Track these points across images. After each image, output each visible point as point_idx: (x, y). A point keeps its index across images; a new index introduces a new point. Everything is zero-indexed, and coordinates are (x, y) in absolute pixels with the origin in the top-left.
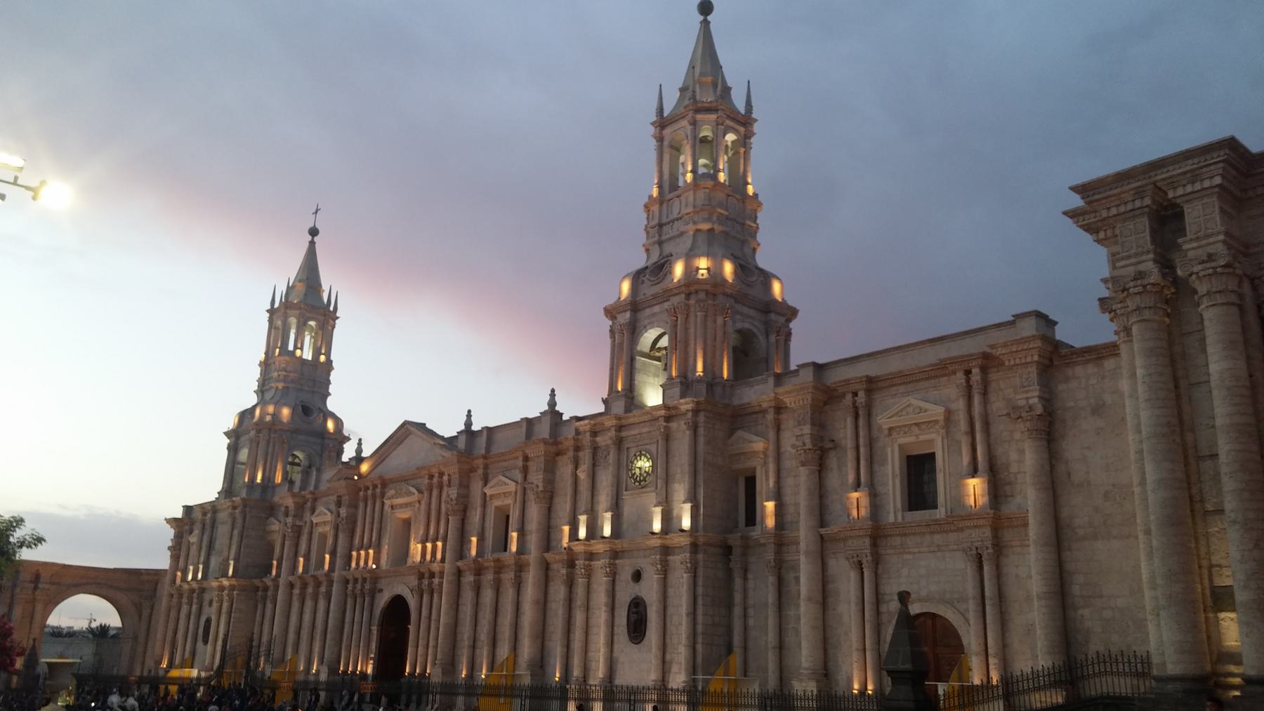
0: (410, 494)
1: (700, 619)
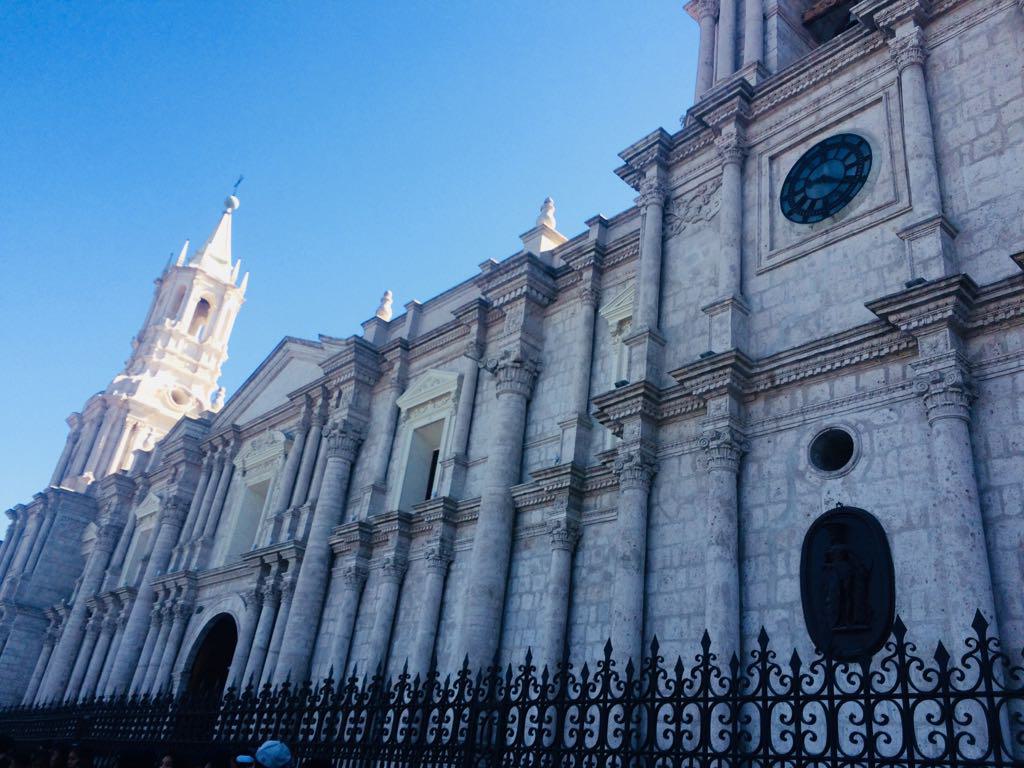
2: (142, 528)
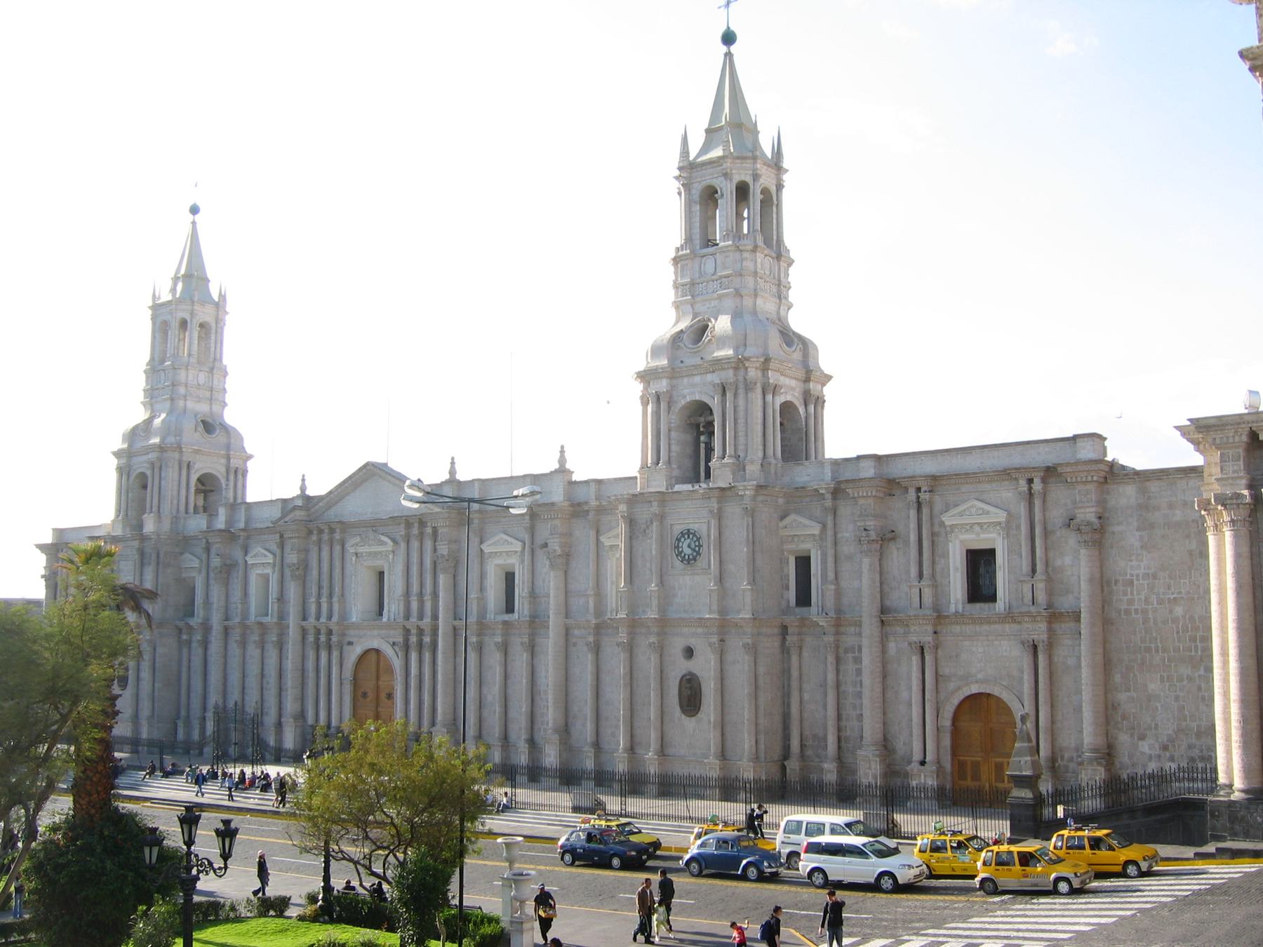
0: (383, 543)
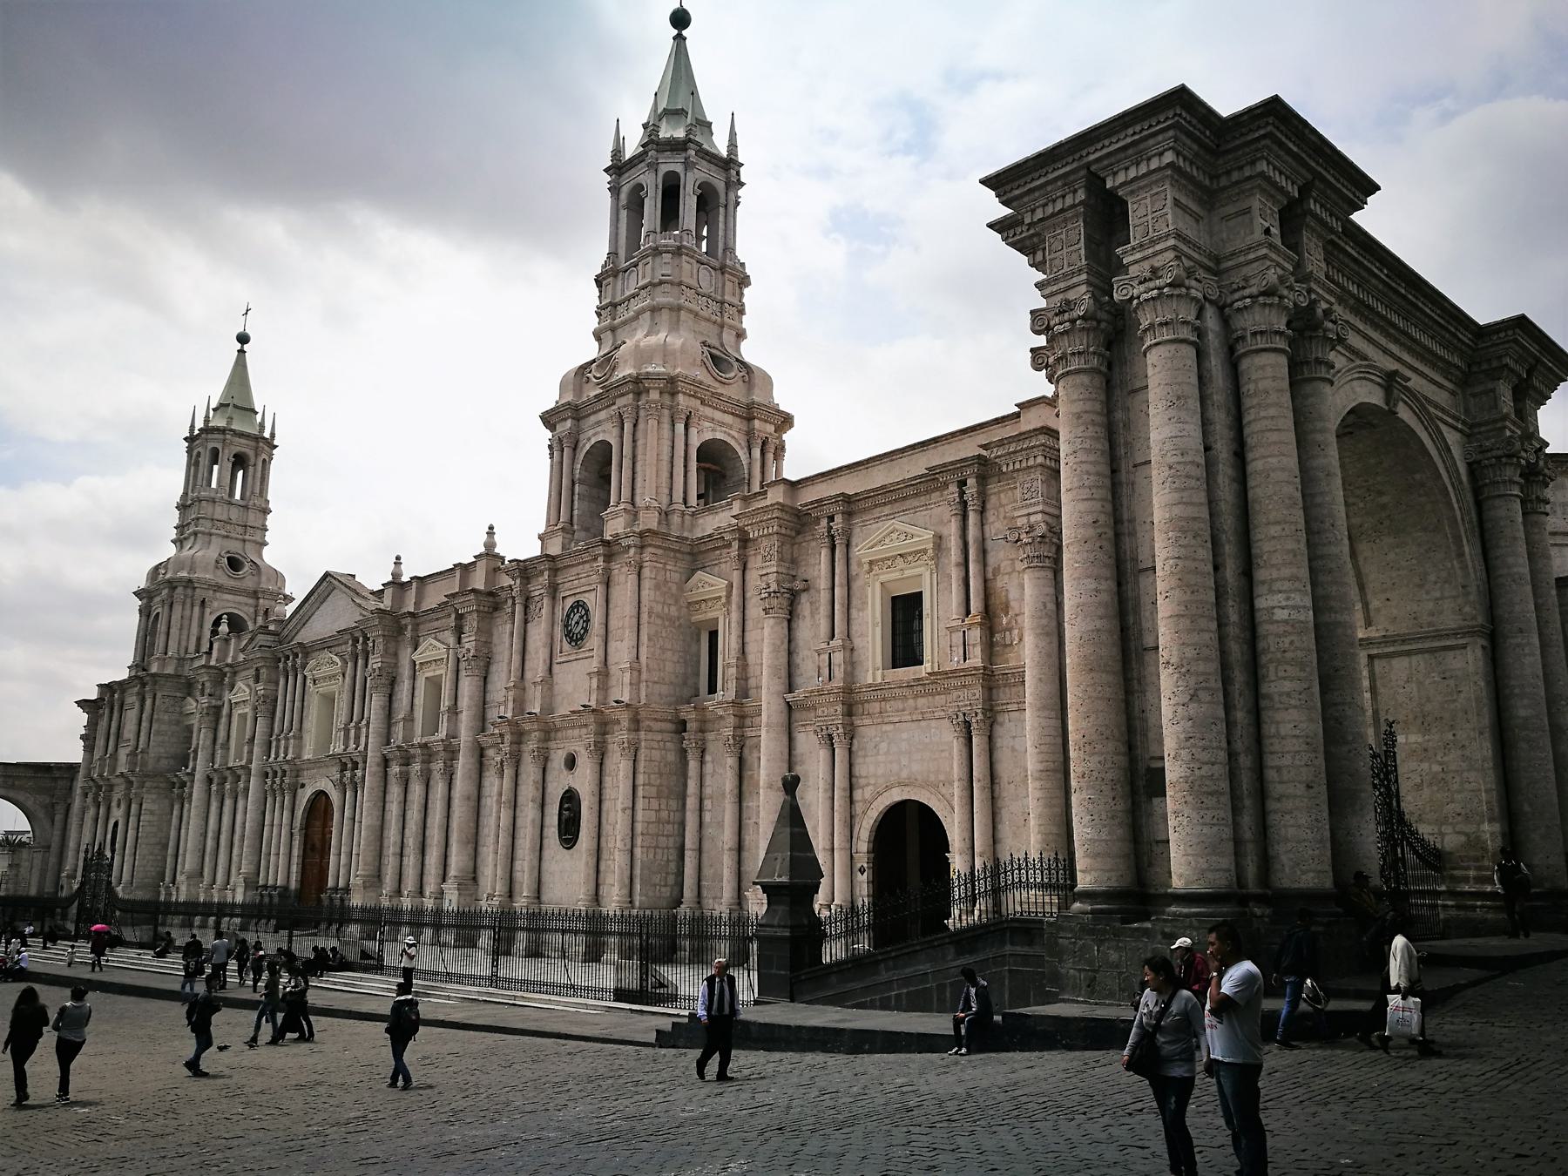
1: (639, 816)
2: (237, 712)
